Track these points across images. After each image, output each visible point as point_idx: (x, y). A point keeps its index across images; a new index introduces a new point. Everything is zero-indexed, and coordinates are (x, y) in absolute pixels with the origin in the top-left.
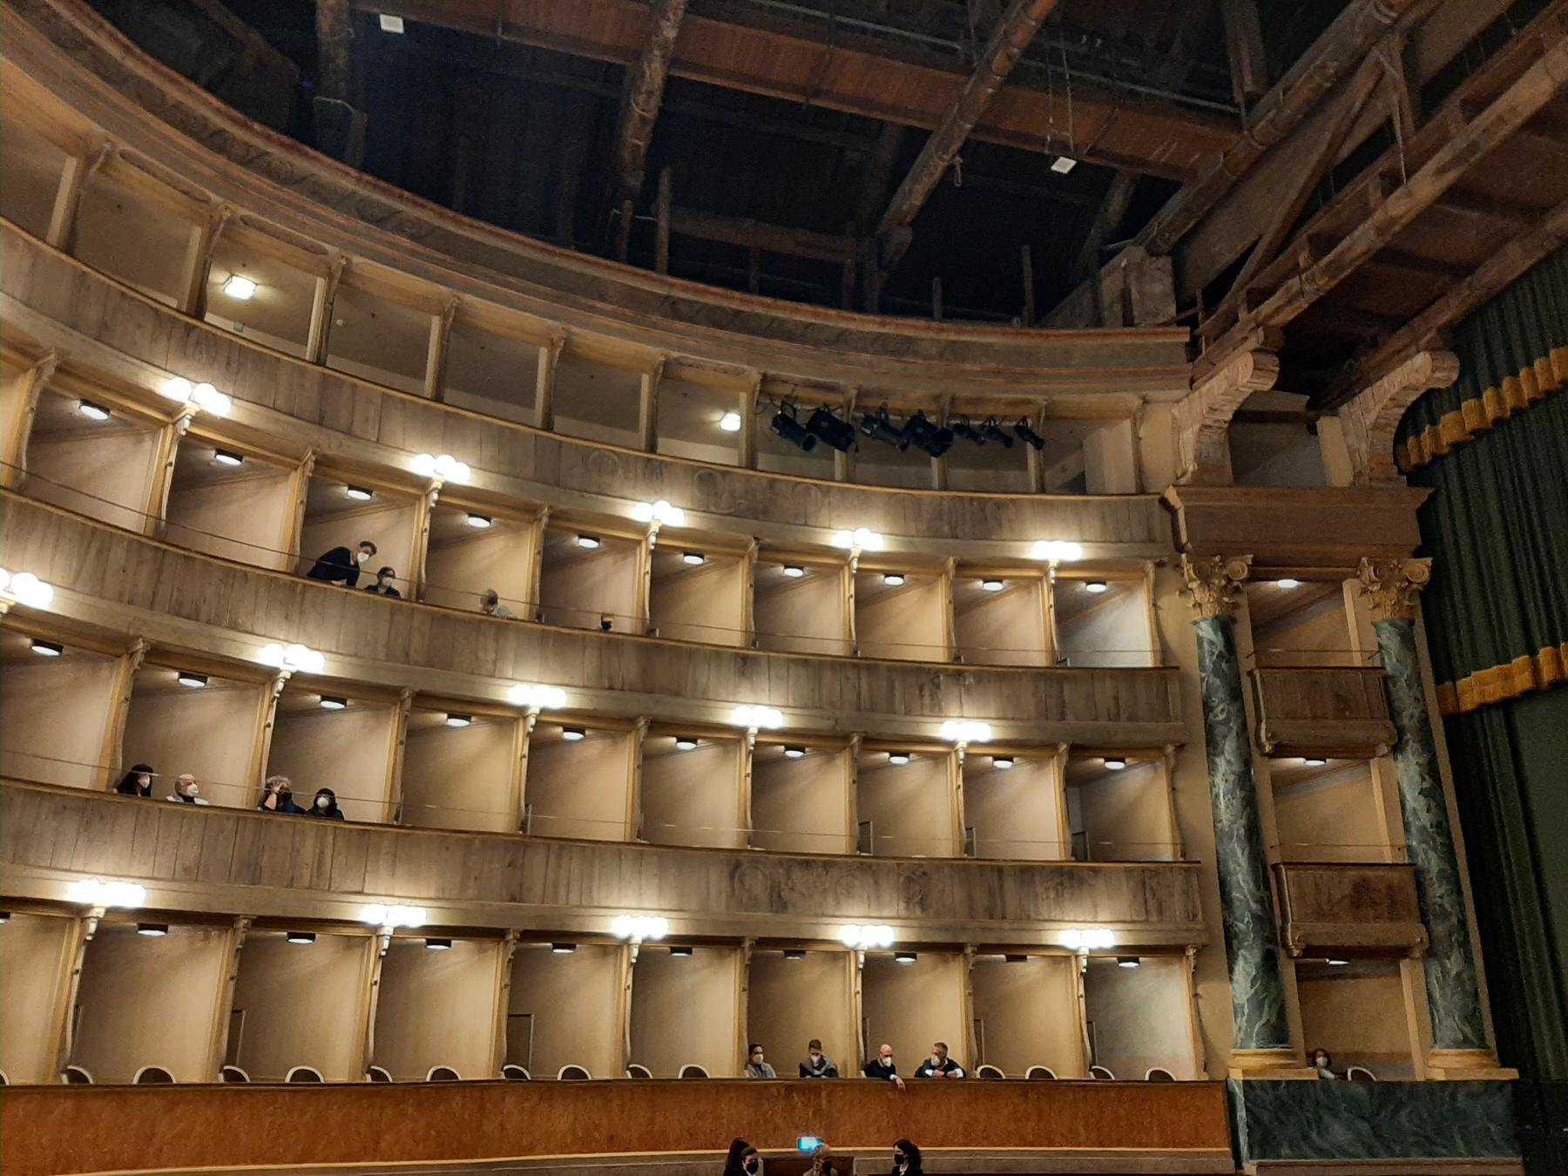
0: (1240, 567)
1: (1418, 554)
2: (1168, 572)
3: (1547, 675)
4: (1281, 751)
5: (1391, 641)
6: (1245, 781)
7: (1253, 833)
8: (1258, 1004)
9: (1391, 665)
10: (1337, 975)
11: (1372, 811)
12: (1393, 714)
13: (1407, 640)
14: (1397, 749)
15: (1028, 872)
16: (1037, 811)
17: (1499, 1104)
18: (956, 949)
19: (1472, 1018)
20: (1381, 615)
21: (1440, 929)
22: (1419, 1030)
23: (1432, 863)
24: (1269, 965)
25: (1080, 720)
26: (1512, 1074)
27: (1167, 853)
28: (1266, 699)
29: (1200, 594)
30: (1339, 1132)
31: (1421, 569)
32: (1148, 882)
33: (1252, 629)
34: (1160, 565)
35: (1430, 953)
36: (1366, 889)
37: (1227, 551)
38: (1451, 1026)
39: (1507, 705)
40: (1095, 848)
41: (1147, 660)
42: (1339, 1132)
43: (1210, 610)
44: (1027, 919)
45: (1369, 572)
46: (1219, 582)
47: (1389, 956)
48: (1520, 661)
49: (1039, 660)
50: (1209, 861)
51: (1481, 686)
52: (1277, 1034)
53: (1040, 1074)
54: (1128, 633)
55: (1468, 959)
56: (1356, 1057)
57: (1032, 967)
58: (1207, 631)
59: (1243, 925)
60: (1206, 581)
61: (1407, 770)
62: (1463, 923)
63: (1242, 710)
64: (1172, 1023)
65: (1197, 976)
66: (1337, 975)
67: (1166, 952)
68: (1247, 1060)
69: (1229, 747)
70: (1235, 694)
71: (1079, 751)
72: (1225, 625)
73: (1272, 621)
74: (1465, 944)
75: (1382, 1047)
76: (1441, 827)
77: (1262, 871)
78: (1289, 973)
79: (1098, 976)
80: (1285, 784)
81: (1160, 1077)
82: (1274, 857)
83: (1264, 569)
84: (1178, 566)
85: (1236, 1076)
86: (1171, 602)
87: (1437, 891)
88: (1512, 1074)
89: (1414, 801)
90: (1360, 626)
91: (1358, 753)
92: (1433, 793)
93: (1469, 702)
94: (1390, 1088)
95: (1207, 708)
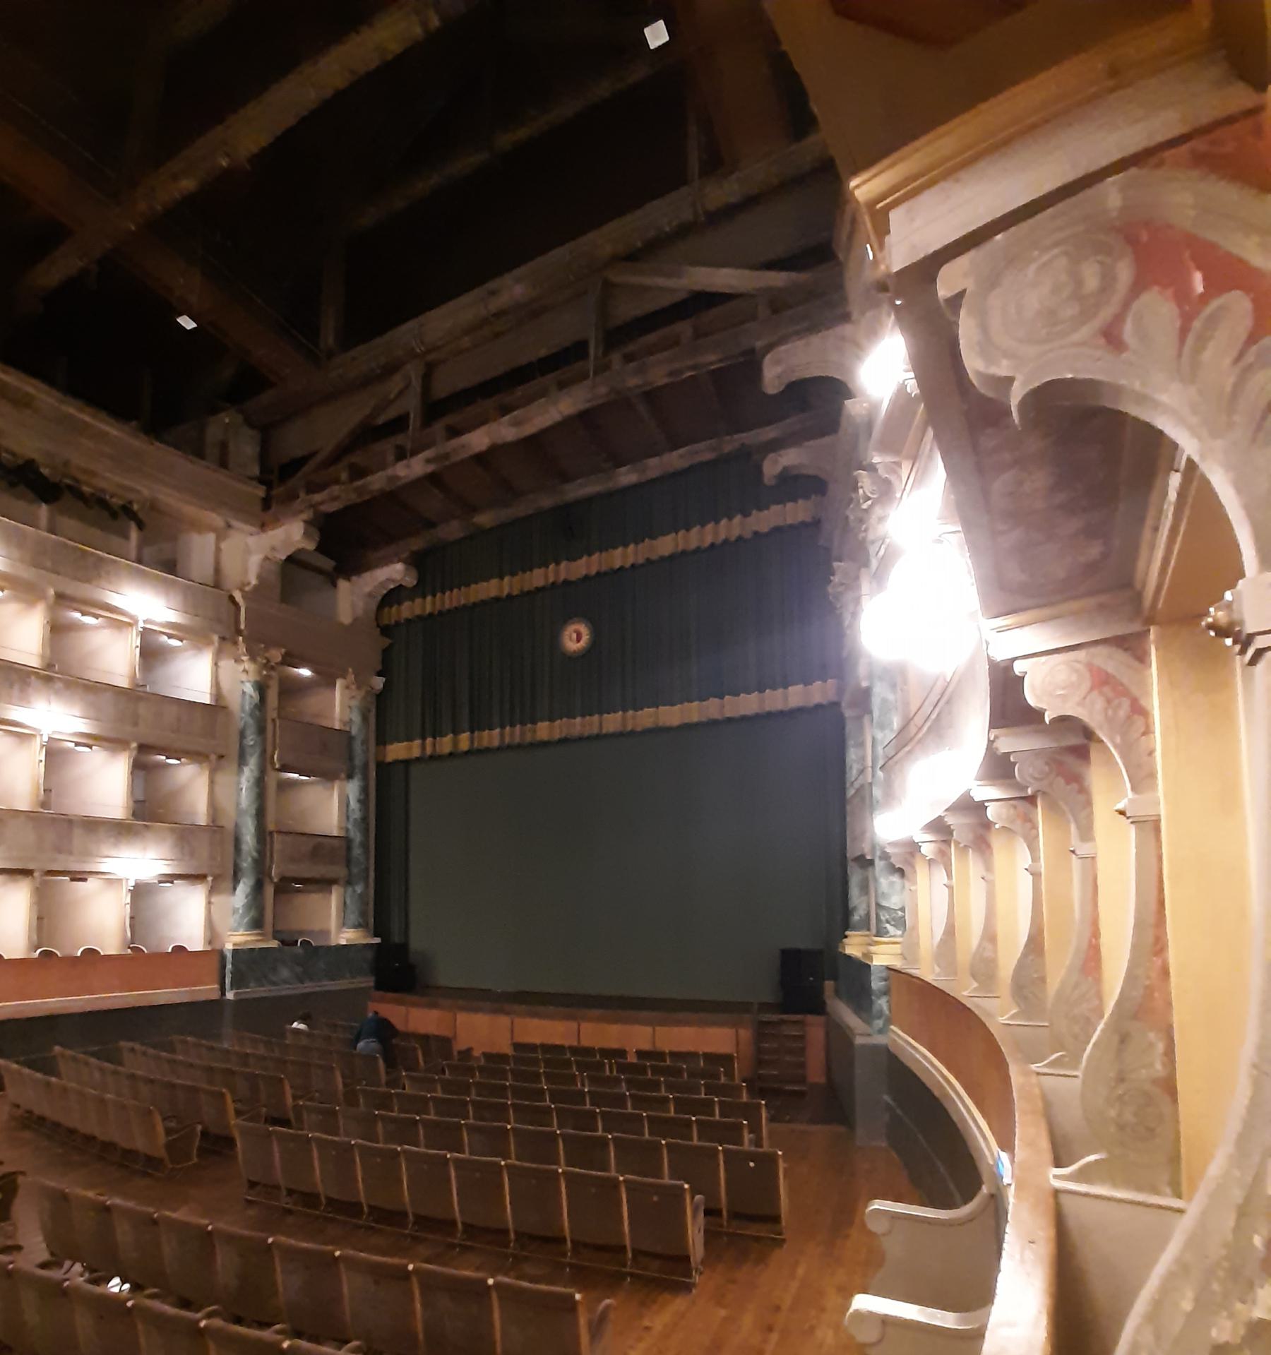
0: (276, 655)
1: (379, 674)
2: (228, 646)
3: (429, 751)
4: (285, 768)
5: (356, 718)
6: (260, 783)
7: (260, 814)
8: (248, 907)
9: (354, 731)
10: (298, 891)
11: (329, 807)
12: (351, 758)
13: (365, 718)
14: (350, 777)
15: (94, 826)
16: (107, 783)
17: (370, 955)
18: (26, 873)
19: (363, 914)
20: (354, 703)
21: (355, 870)
22: (335, 921)
23: (357, 837)
24: (258, 888)
25: (148, 727)
26: (377, 940)
27: (202, 818)
28: (280, 736)
29: (248, 665)
30: (285, 973)
31: (379, 683)
32: (185, 835)
33: (277, 695)
34: (223, 639)
35: (349, 882)
36: (320, 847)
37: (270, 643)
38: (353, 917)
39: (407, 763)
40: (150, 811)
41: (206, 699)
42: (285, 973)
43: (253, 677)
44: (87, 854)
45: (351, 677)
46: (262, 661)
47: (324, 884)
48: (417, 742)
49: (123, 683)
50: (229, 824)
51: (397, 751)
52: (257, 924)
53: (90, 952)
54: (194, 676)
55: (367, 886)
56: (301, 933)
57: (92, 884)
58: (249, 689)
59: (246, 863)
60: (253, 659)
61: (353, 788)
62: (367, 869)
63: (264, 742)
64: (191, 919)
65: (212, 891)
66: (298, 891)
67: (194, 878)
68: (236, 938)
69: (253, 762)
70: (261, 730)
71: (144, 748)
72: (261, 688)
73: (291, 689)
74: (366, 878)
75: (317, 927)
76: (365, 819)
77: (263, 835)
78: (269, 891)
79: (140, 893)
80: (285, 786)
81: (180, 949)
82: (271, 826)
83: (292, 659)
84: (235, 643)
85: (229, 947)
86: (227, 664)
87: (357, 851)
88: (377, 940)
89: (354, 804)
90: (340, 706)
91: (328, 776)
92: (363, 802)
93: (390, 757)
94: (317, 948)
95: (242, 735)
